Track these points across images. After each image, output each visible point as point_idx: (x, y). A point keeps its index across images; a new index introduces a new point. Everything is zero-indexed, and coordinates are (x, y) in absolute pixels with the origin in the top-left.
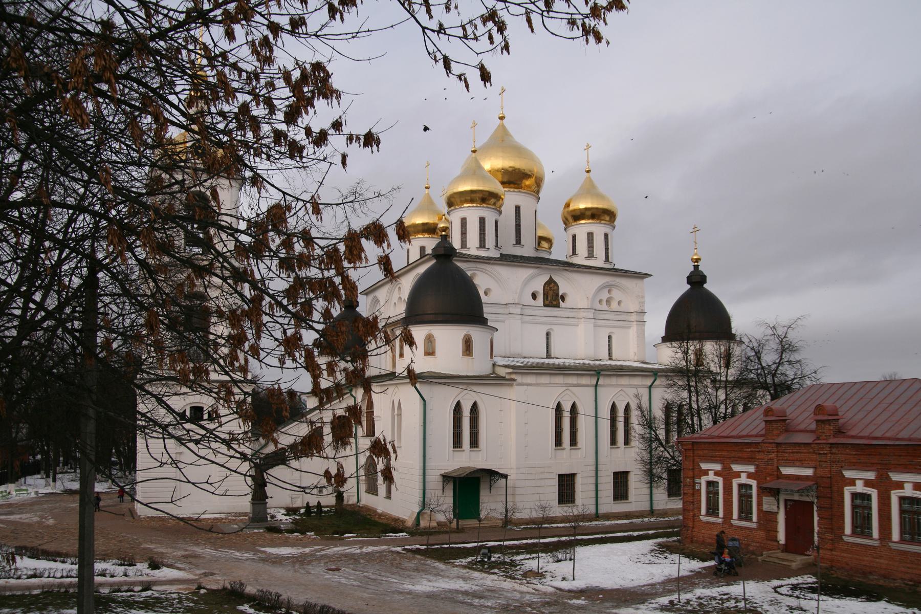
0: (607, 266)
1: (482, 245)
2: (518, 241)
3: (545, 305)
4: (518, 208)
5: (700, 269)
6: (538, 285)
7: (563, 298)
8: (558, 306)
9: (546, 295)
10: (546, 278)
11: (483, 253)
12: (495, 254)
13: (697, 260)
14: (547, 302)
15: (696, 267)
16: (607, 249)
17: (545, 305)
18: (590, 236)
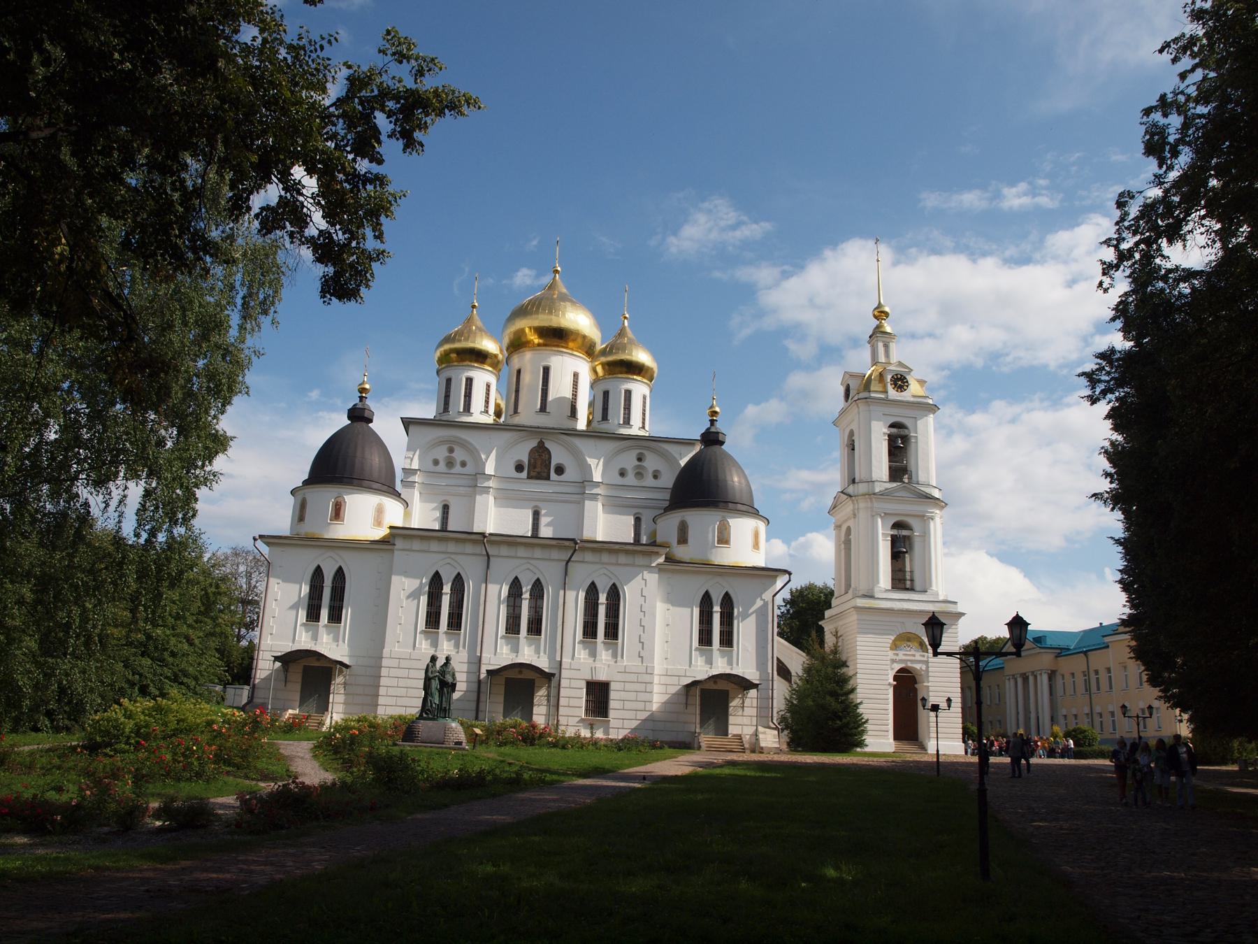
3: (529, 477)
6: (523, 452)
7: (560, 470)
8: (548, 478)
9: (532, 466)
10: (533, 443)
14: (533, 474)
16: (644, 414)
17: (529, 477)
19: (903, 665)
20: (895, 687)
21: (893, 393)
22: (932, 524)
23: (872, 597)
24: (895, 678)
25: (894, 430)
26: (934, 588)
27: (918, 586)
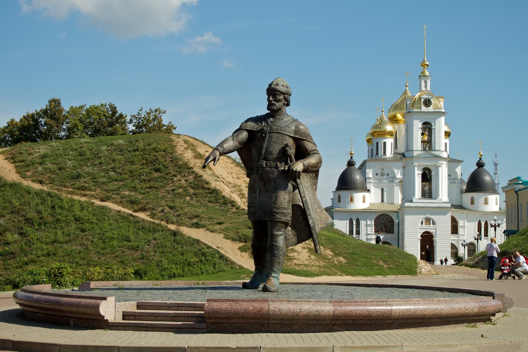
19: (425, 230)
20: (421, 240)
21: (424, 109)
22: (440, 168)
23: (411, 201)
24: (422, 236)
25: (425, 126)
26: (440, 197)
27: (433, 196)
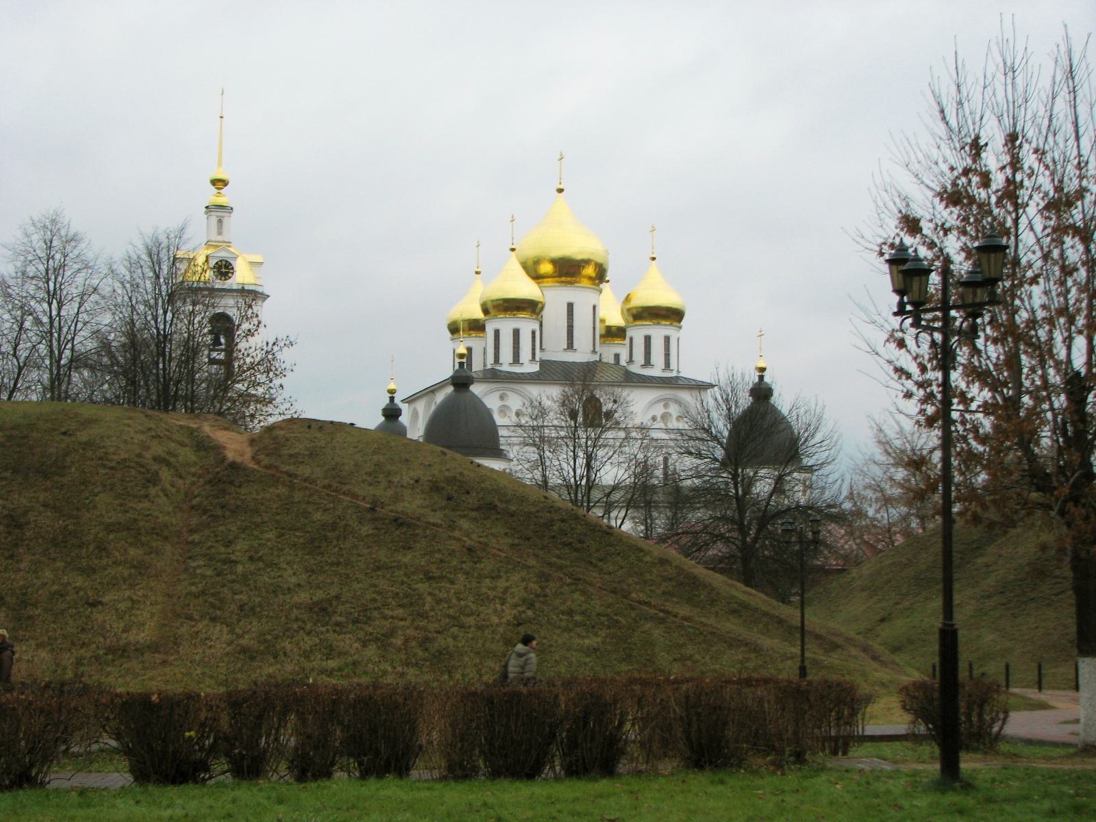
0: (668, 374)
1: (516, 359)
2: (570, 345)
4: (570, 306)
5: (766, 379)
11: (517, 369)
12: (535, 368)
13: (762, 370)
15: (761, 378)
18: (648, 339)
